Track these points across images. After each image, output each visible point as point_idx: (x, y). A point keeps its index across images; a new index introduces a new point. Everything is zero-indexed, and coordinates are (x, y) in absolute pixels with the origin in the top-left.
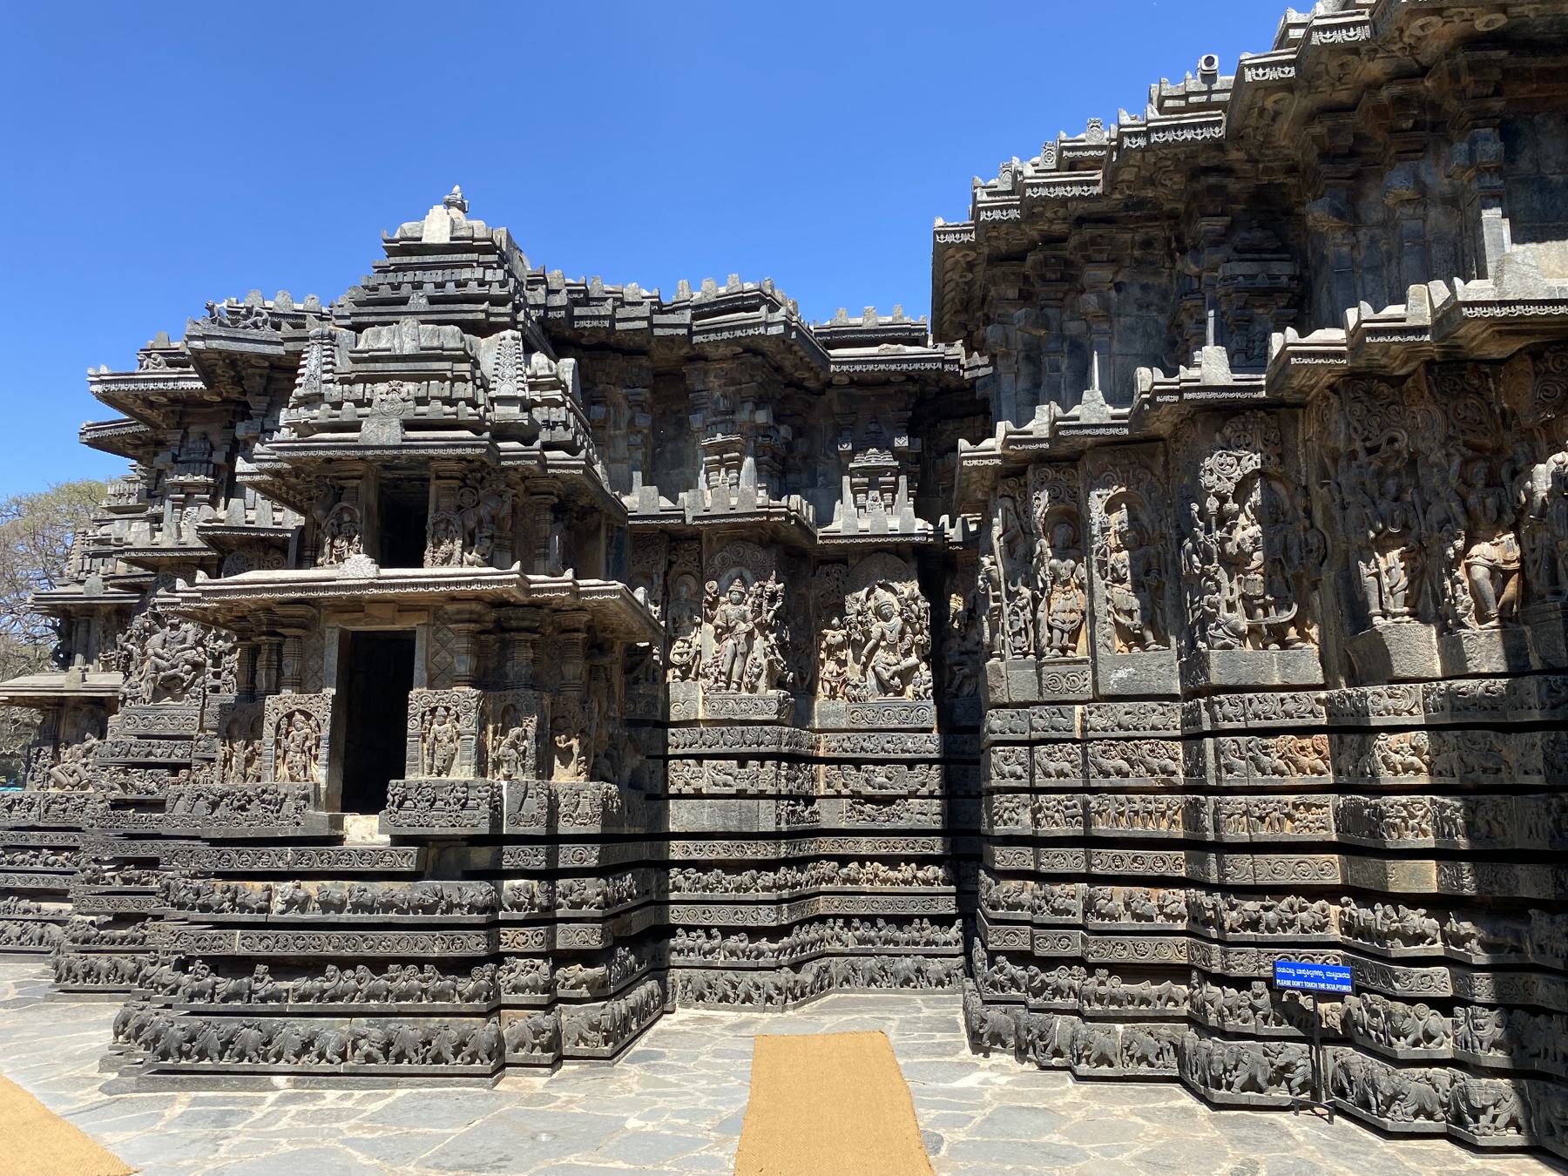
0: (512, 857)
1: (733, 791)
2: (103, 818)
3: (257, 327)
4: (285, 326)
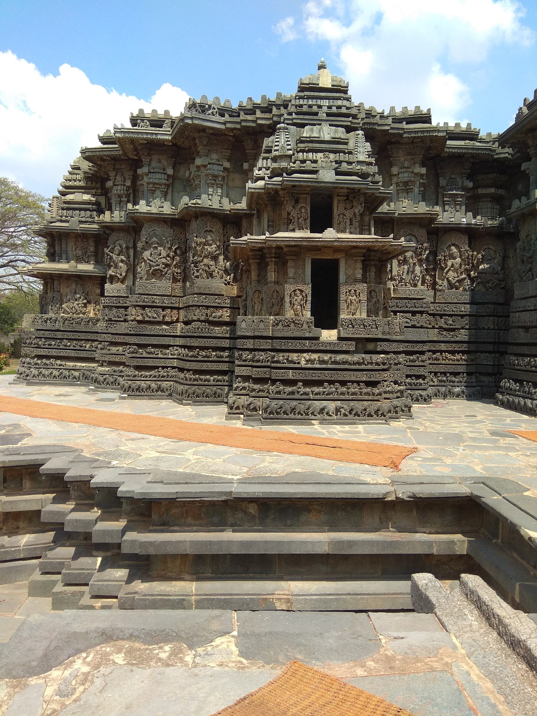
0: (381, 346)
1: (410, 325)
2: (136, 327)
3: (214, 115)
4: (227, 116)
